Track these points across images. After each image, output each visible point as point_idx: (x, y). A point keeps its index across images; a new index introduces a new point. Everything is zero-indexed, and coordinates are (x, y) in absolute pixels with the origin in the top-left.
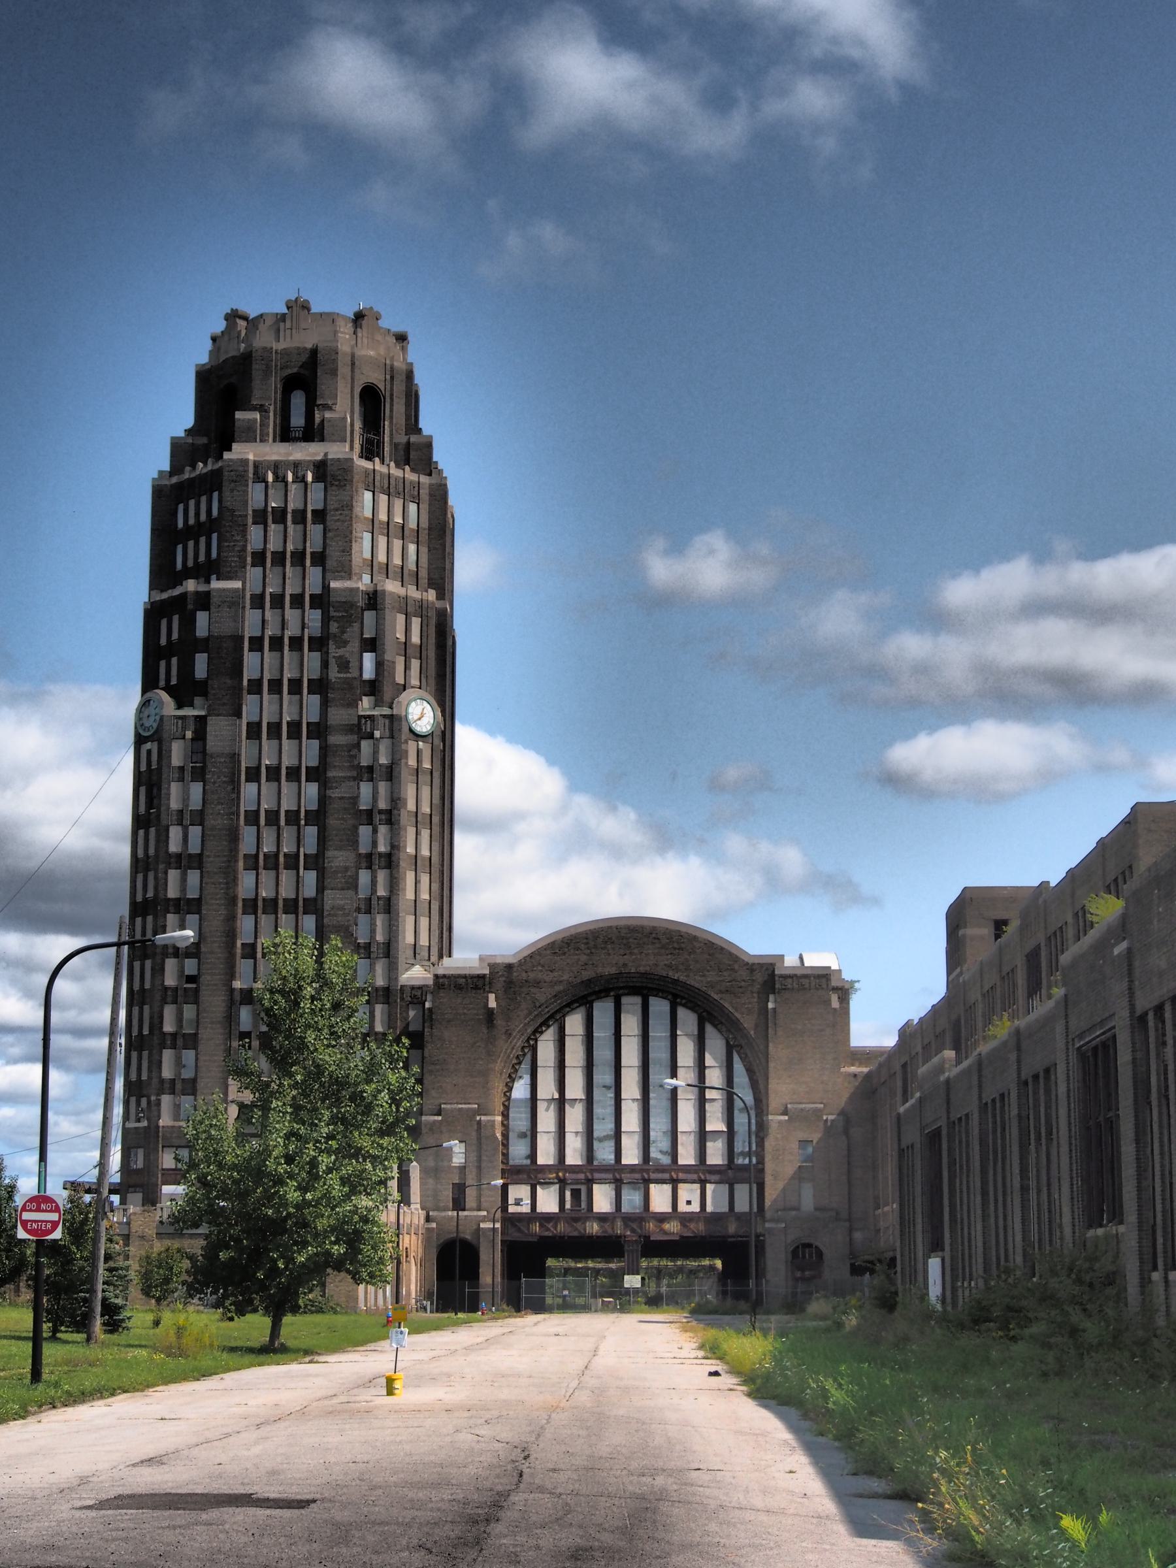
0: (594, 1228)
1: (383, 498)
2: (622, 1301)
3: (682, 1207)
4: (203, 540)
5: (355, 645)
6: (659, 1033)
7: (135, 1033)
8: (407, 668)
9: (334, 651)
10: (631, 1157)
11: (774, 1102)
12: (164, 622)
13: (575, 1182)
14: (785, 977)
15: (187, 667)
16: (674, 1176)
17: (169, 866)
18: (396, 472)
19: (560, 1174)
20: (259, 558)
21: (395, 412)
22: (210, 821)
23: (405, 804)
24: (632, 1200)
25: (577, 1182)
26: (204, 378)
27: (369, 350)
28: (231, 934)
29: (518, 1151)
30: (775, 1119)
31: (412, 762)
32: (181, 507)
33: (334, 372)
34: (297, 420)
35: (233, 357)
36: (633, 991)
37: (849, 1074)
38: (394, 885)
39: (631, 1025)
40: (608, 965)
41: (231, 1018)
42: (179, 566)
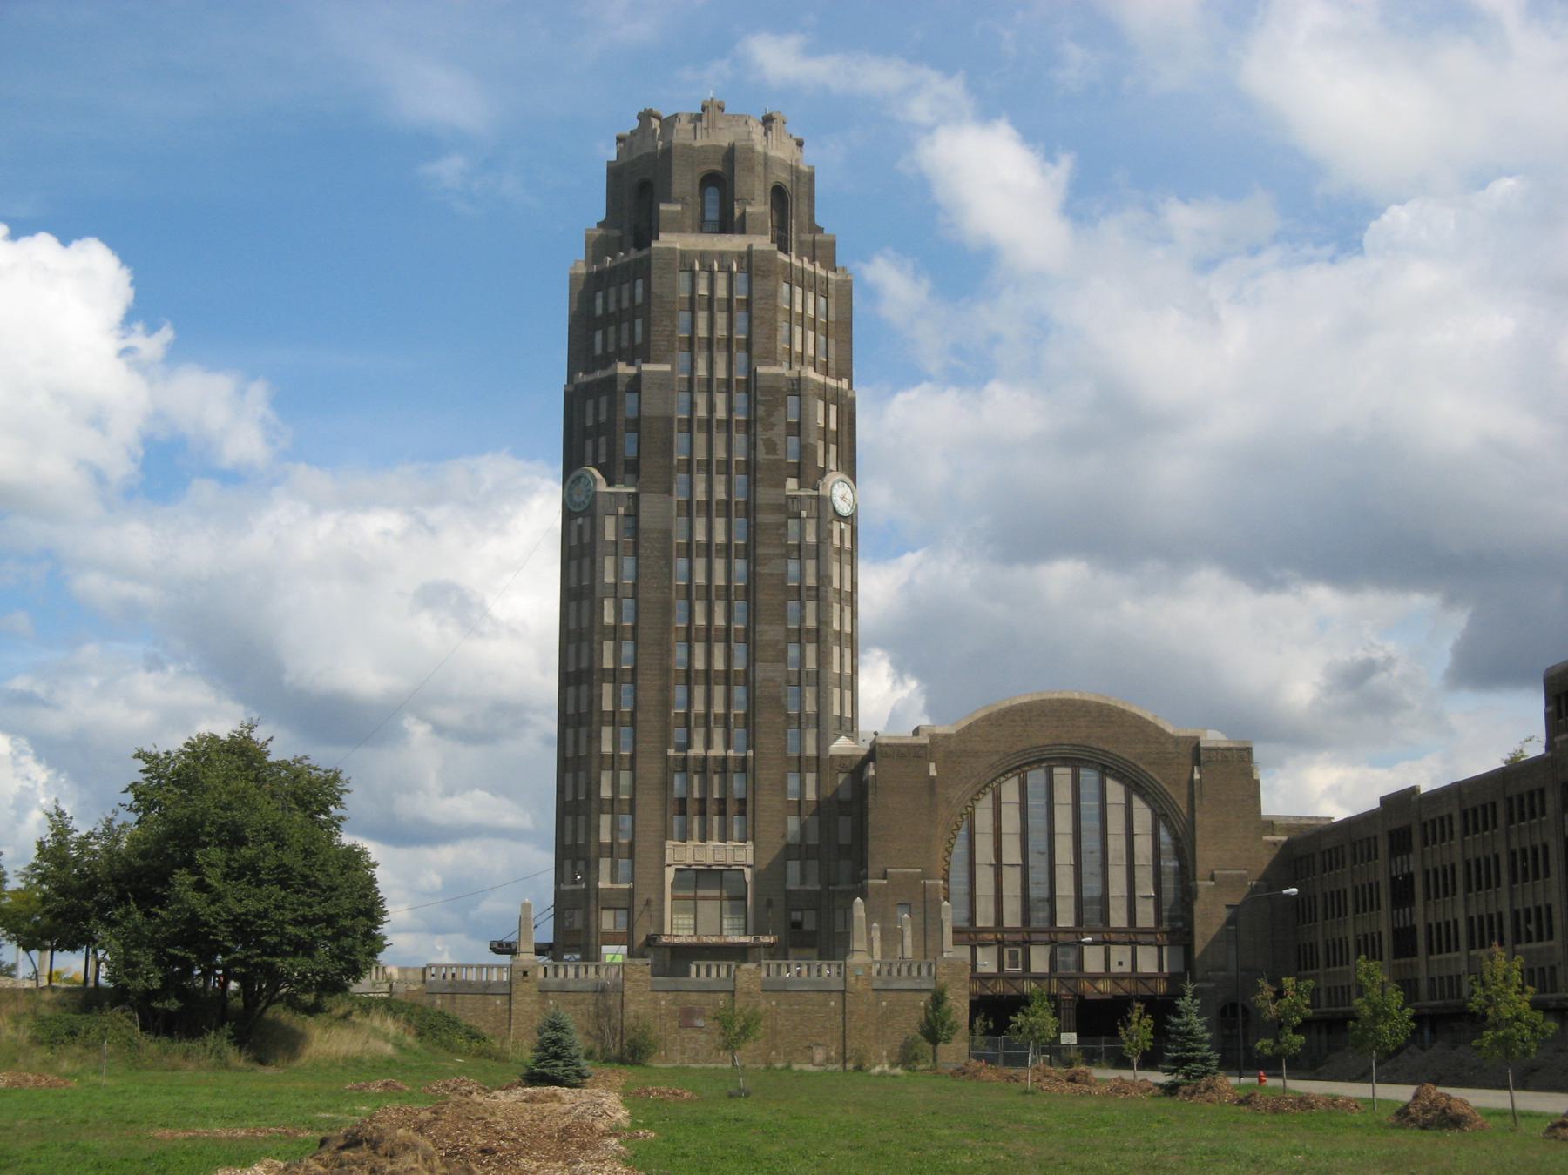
1: (798, 291)
3: (1115, 968)
4: (625, 326)
5: (781, 429)
7: (569, 797)
8: (826, 452)
9: (762, 434)
10: (1066, 919)
11: (1202, 868)
12: (590, 404)
14: (1209, 749)
17: (604, 637)
18: (809, 267)
21: (797, 208)
23: (831, 582)
25: (1015, 944)
27: (780, 150)
28: (666, 704)
30: (1203, 884)
31: (836, 542)
32: (600, 295)
33: (751, 170)
34: (713, 215)
36: (1064, 761)
37: (1269, 843)
41: (666, 785)
42: (598, 351)
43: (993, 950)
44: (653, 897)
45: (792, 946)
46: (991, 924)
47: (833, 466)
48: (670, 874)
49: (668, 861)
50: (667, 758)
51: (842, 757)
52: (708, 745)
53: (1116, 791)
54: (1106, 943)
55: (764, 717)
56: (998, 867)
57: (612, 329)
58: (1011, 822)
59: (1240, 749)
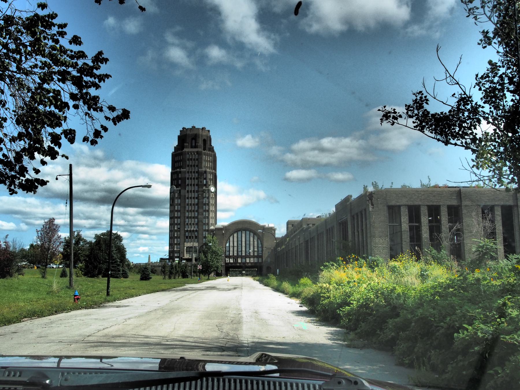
0: (238, 265)
2: (242, 275)
6: (248, 236)
9: (200, 180)
11: (264, 246)
13: (235, 258)
15: (178, 182)
16: (250, 257)
19: (233, 257)
20: (188, 166)
22: (182, 205)
24: (244, 260)
26: (179, 137)
28: (185, 222)
29: (227, 253)
30: (264, 249)
34: (194, 144)
38: (209, 215)
39: (244, 235)
40: (240, 226)
41: (185, 234)
53: (252, 234)
55: (200, 223)
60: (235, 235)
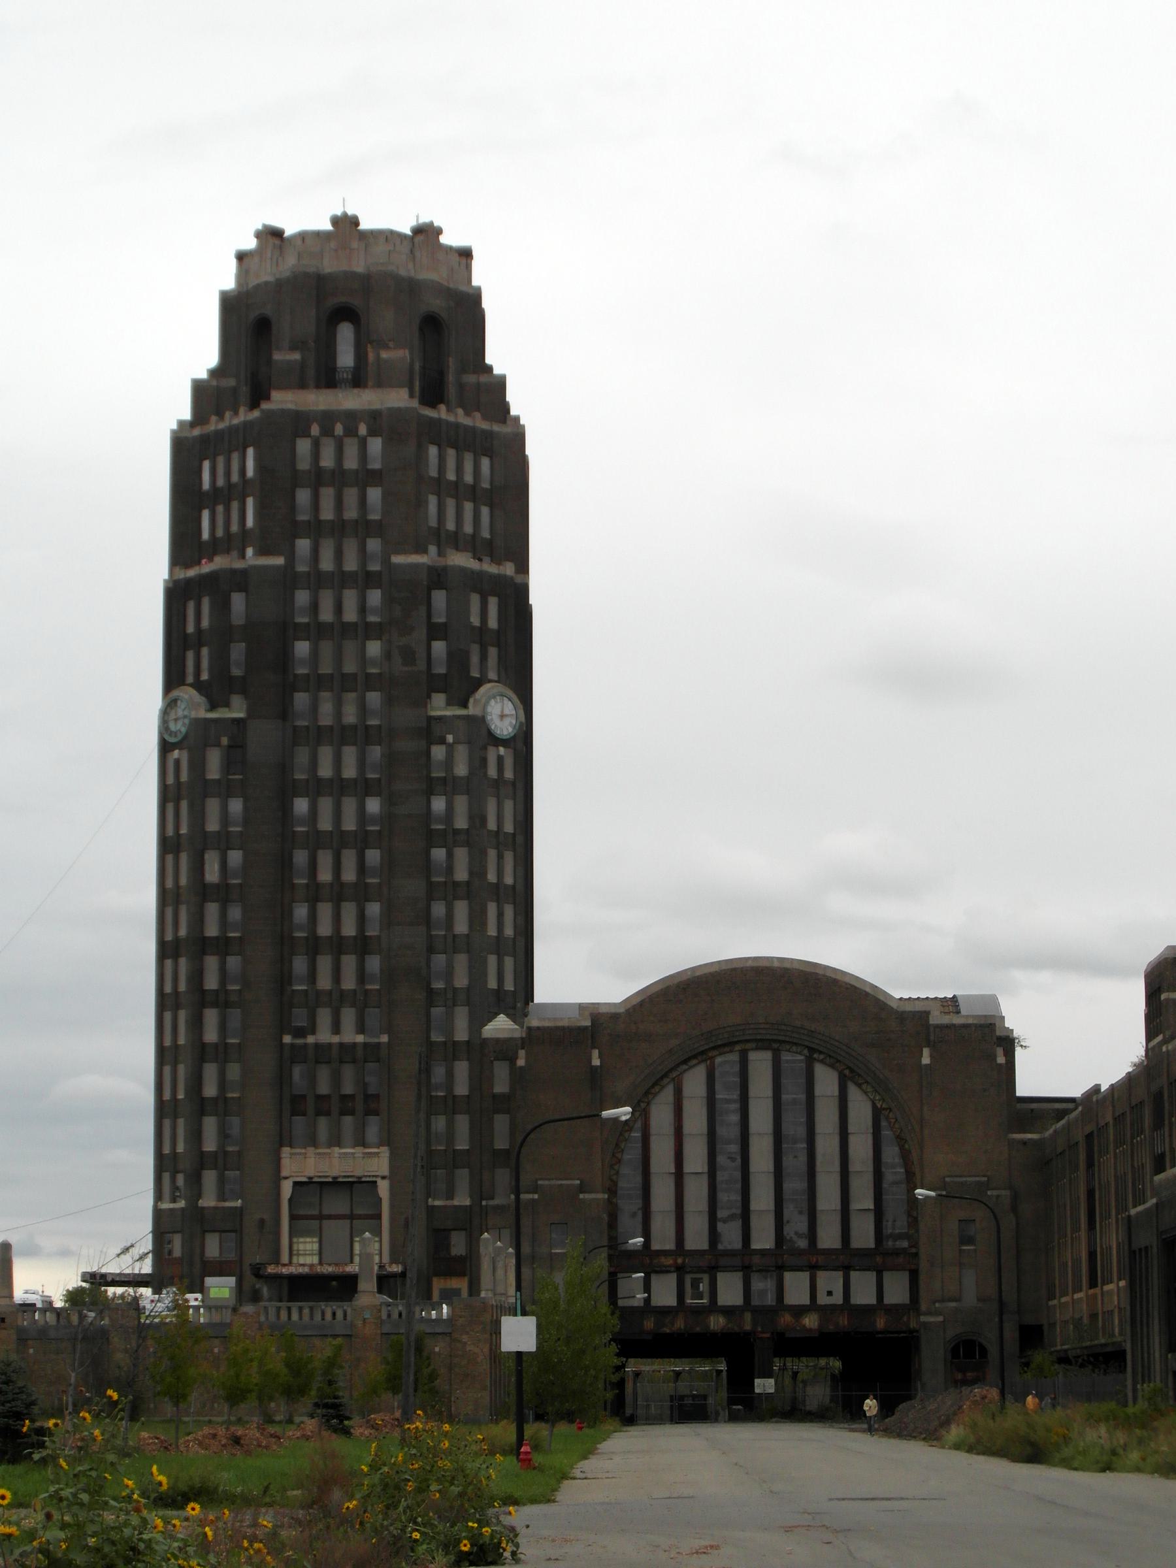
3: (822, 1300)
4: (235, 505)
5: (421, 633)
7: (167, 1096)
10: (763, 1240)
12: (191, 606)
16: (813, 1261)
26: (230, 305)
28: (283, 979)
32: (206, 465)
35: (266, 283)
36: (762, 1044)
43: (672, 1279)
44: (266, 1217)
45: (437, 1274)
46: (670, 1245)
47: (492, 675)
48: (287, 1189)
49: (284, 1173)
50: (282, 1045)
51: (497, 1040)
52: (336, 1029)
53: (826, 1081)
54: (847, 1269)
56: (679, 1175)
57: (220, 509)
58: (695, 1121)
59: (981, 1026)
60: (695, 1082)
